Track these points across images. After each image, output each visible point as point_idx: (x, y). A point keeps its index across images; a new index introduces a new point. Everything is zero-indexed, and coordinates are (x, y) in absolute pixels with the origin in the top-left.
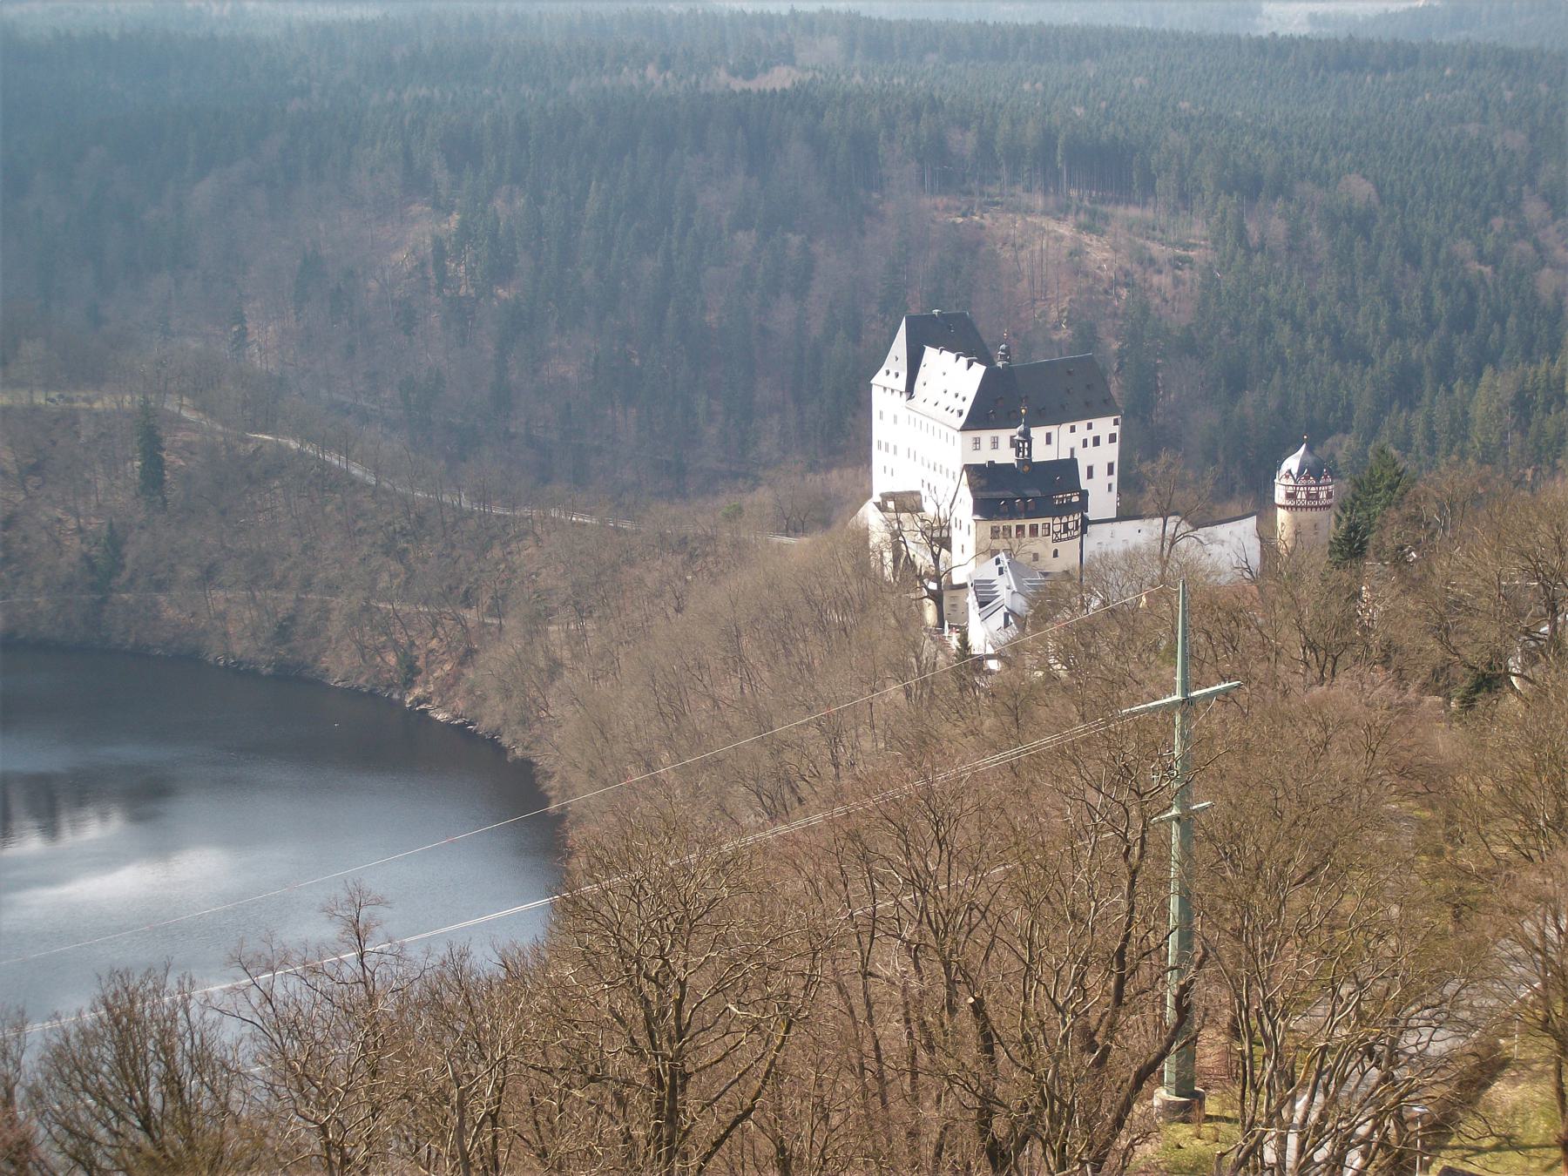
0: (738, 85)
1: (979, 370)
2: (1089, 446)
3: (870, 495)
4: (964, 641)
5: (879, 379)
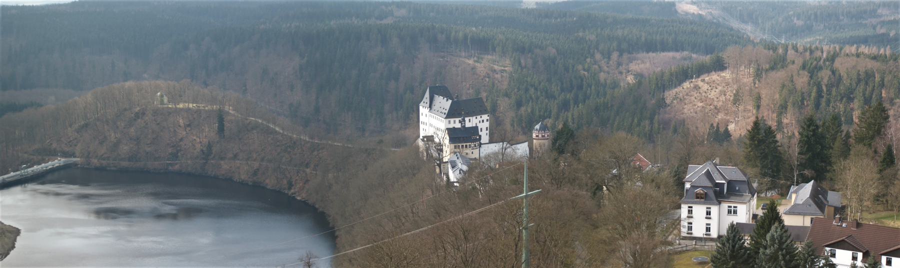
0: (379, 22)
1: (450, 101)
3: (419, 136)
5: (422, 103)
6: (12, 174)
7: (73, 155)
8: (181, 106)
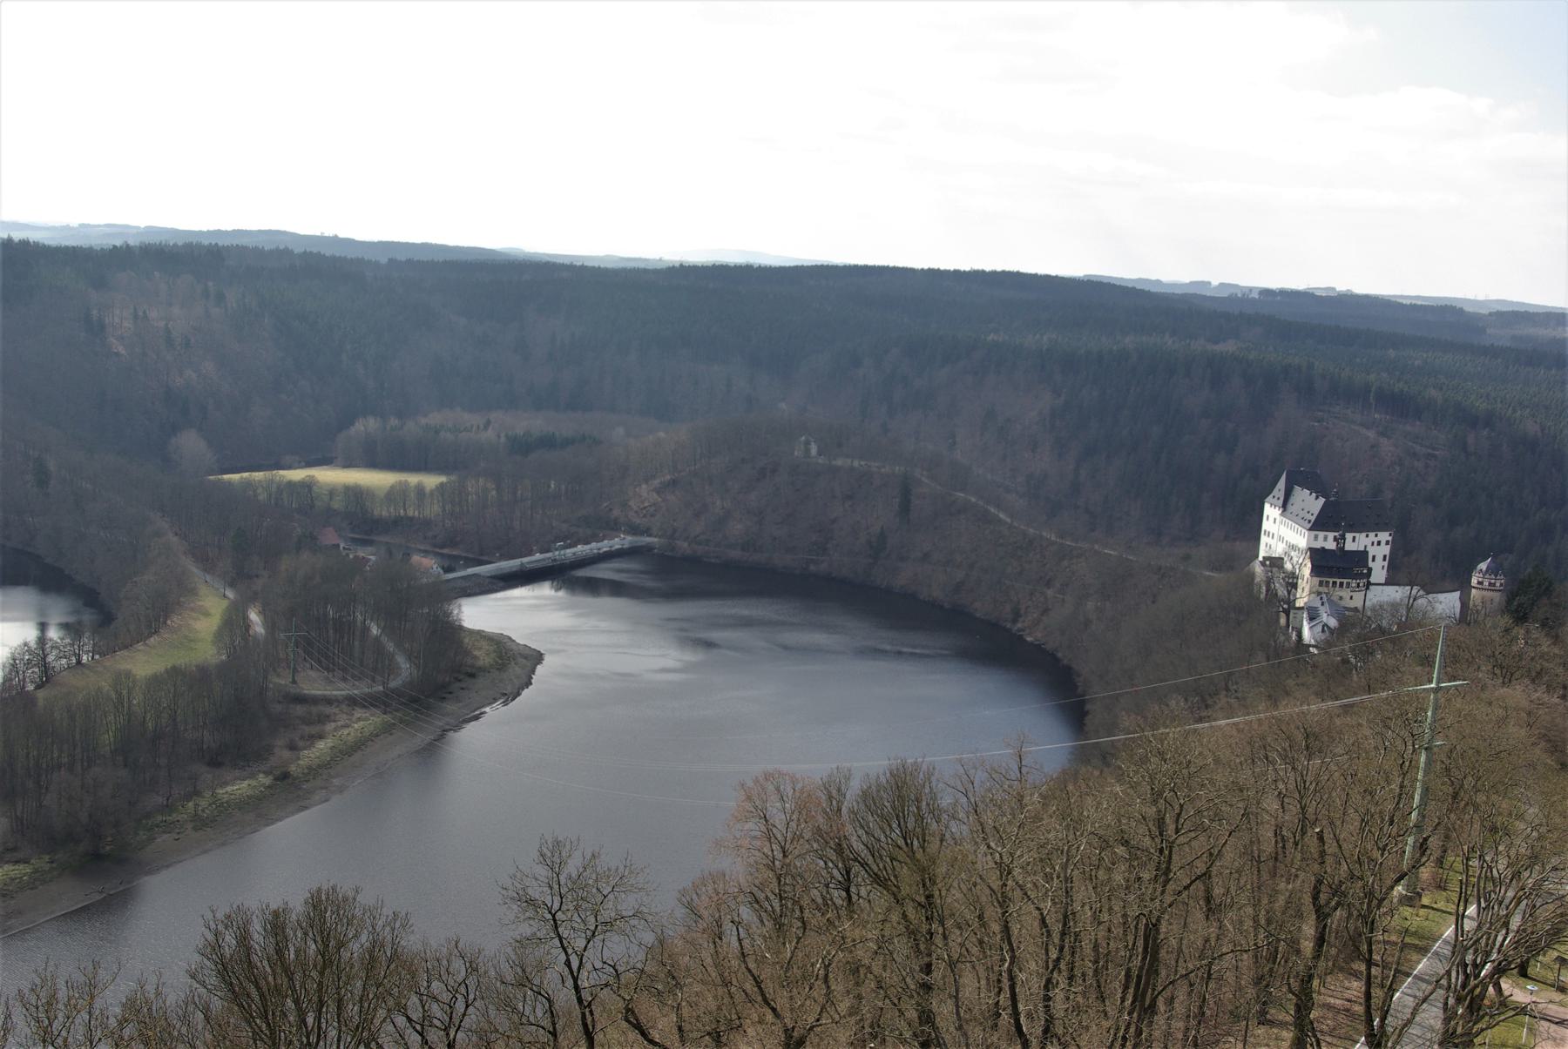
0: (1211, 347)
1: (1322, 500)
2: (1376, 546)
4: (1300, 635)
6: (538, 556)
7: (647, 532)
8: (839, 462)
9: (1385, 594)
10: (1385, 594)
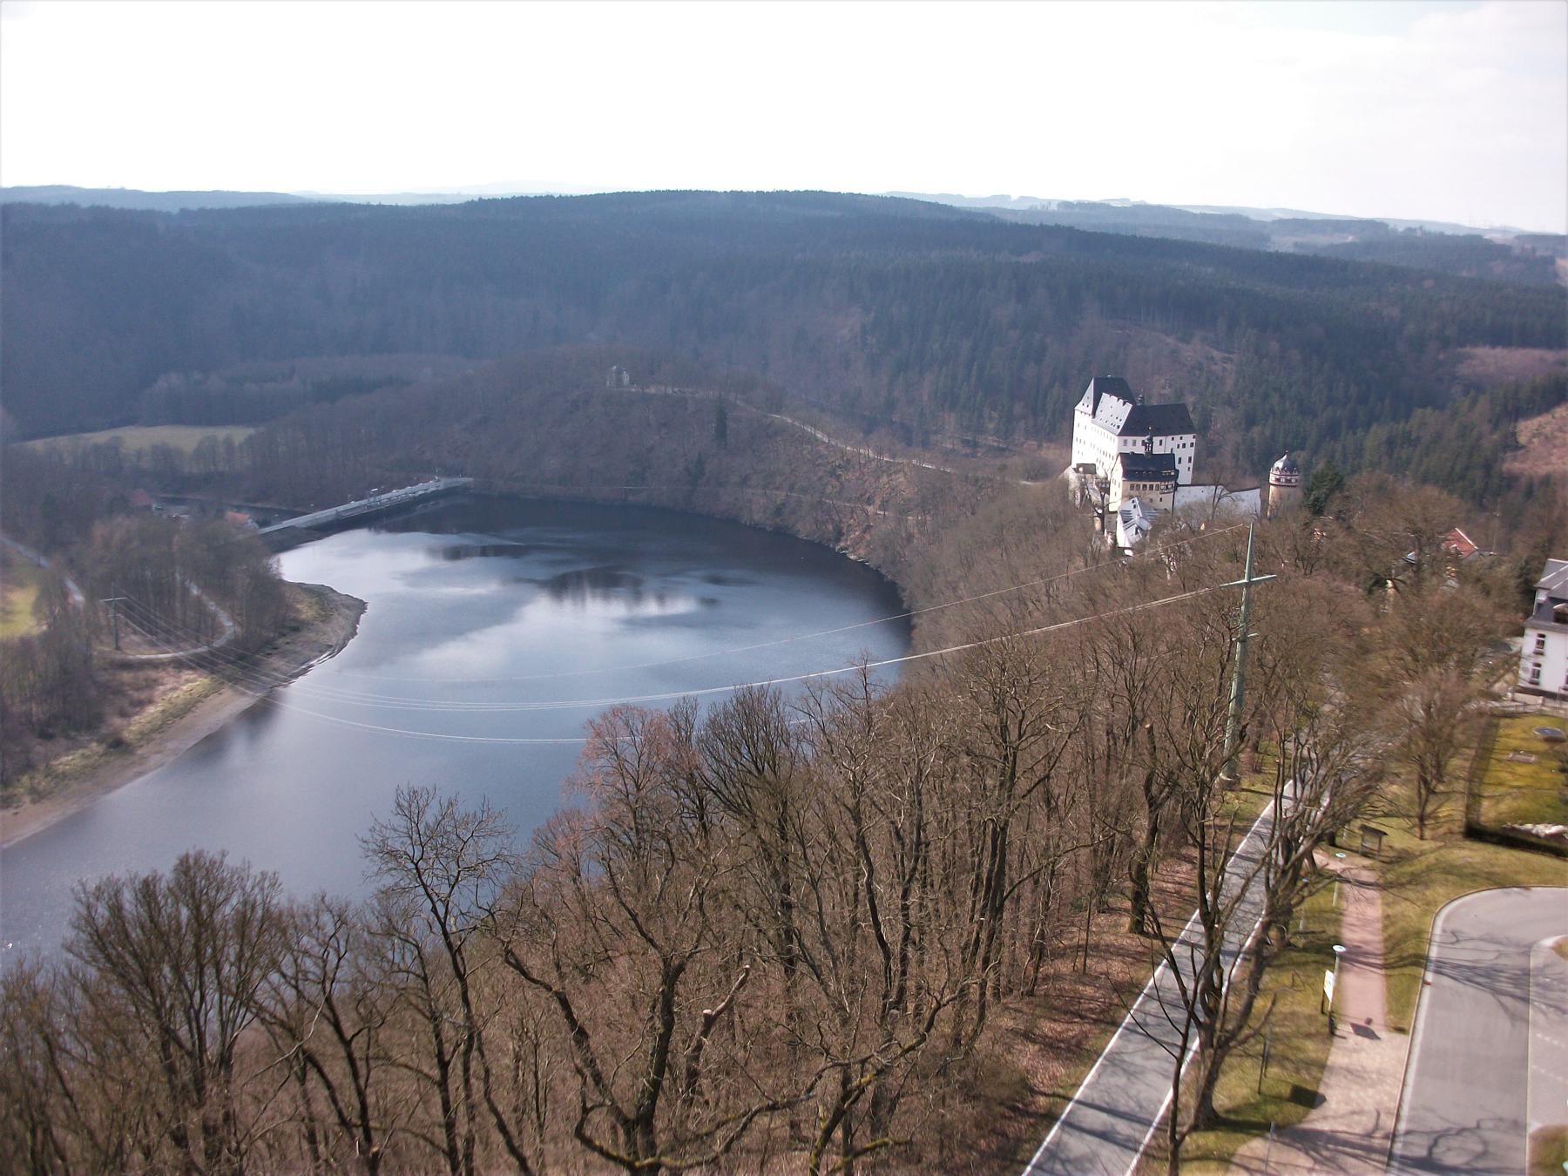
0: (1014, 259)
1: (1129, 406)
4: (1115, 539)
5: (1079, 407)
6: (353, 504)
7: (461, 472)
8: (652, 390)
9: (1193, 495)
10: (1193, 495)
